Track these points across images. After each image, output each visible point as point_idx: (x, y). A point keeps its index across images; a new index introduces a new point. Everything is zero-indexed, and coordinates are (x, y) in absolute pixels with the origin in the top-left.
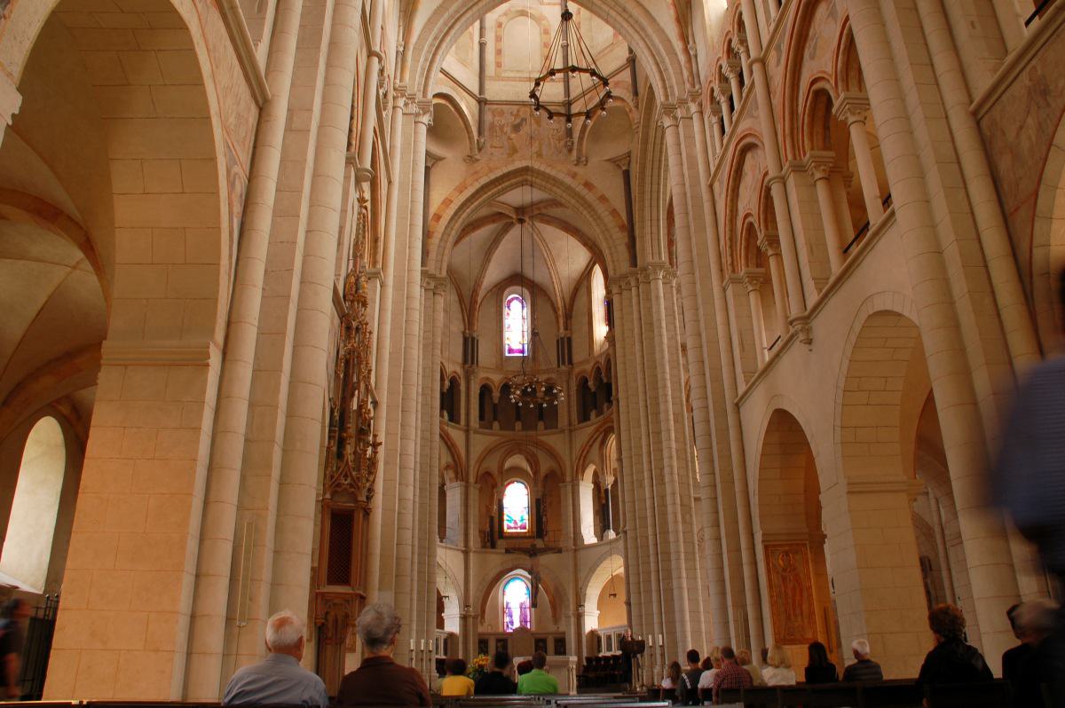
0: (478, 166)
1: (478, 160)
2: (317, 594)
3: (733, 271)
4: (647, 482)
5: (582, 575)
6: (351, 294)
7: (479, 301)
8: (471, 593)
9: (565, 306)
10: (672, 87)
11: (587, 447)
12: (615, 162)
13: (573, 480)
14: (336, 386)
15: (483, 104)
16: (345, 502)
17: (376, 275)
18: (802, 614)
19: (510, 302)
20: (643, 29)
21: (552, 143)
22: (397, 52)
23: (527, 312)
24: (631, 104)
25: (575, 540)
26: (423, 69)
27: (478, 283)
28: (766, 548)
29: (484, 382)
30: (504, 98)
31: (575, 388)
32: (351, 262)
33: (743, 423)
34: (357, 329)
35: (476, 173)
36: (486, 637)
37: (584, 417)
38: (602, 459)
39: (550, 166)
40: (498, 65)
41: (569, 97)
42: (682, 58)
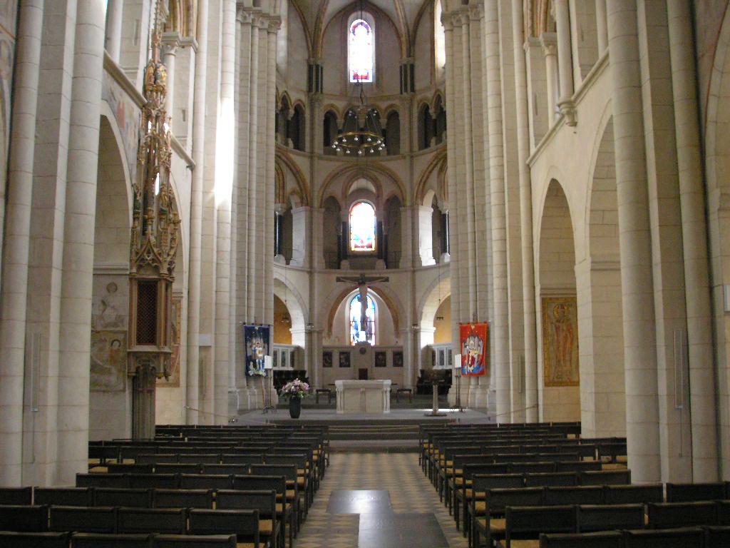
2: (129, 353)
3: (533, 34)
4: (469, 217)
5: (419, 295)
6: (152, 85)
7: (323, 29)
8: (316, 311)
9: (408, 32)
14: (139, 173)
16: (149, 275)
17: (190, 43)
18: (571, 359)
19: (355, 27)
23: (371, 38)
25: (413, 262)
27: (321, 10)
28: (543, 301)
29: (329, 109)
32: (151, 51)
33: (532, 182)
34: (157, 117)
36: (329, 350)
37: (425, 144)
38: (442, 185)
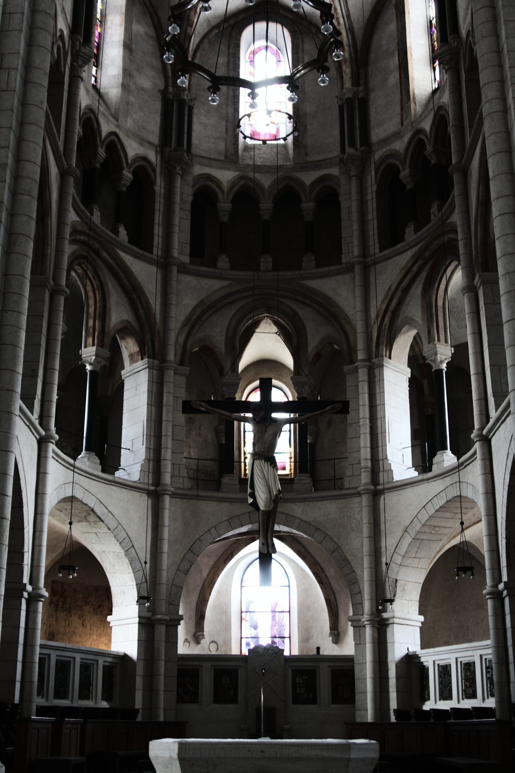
11: (399, 294)
13: (369, 359)
31: (374, 188)
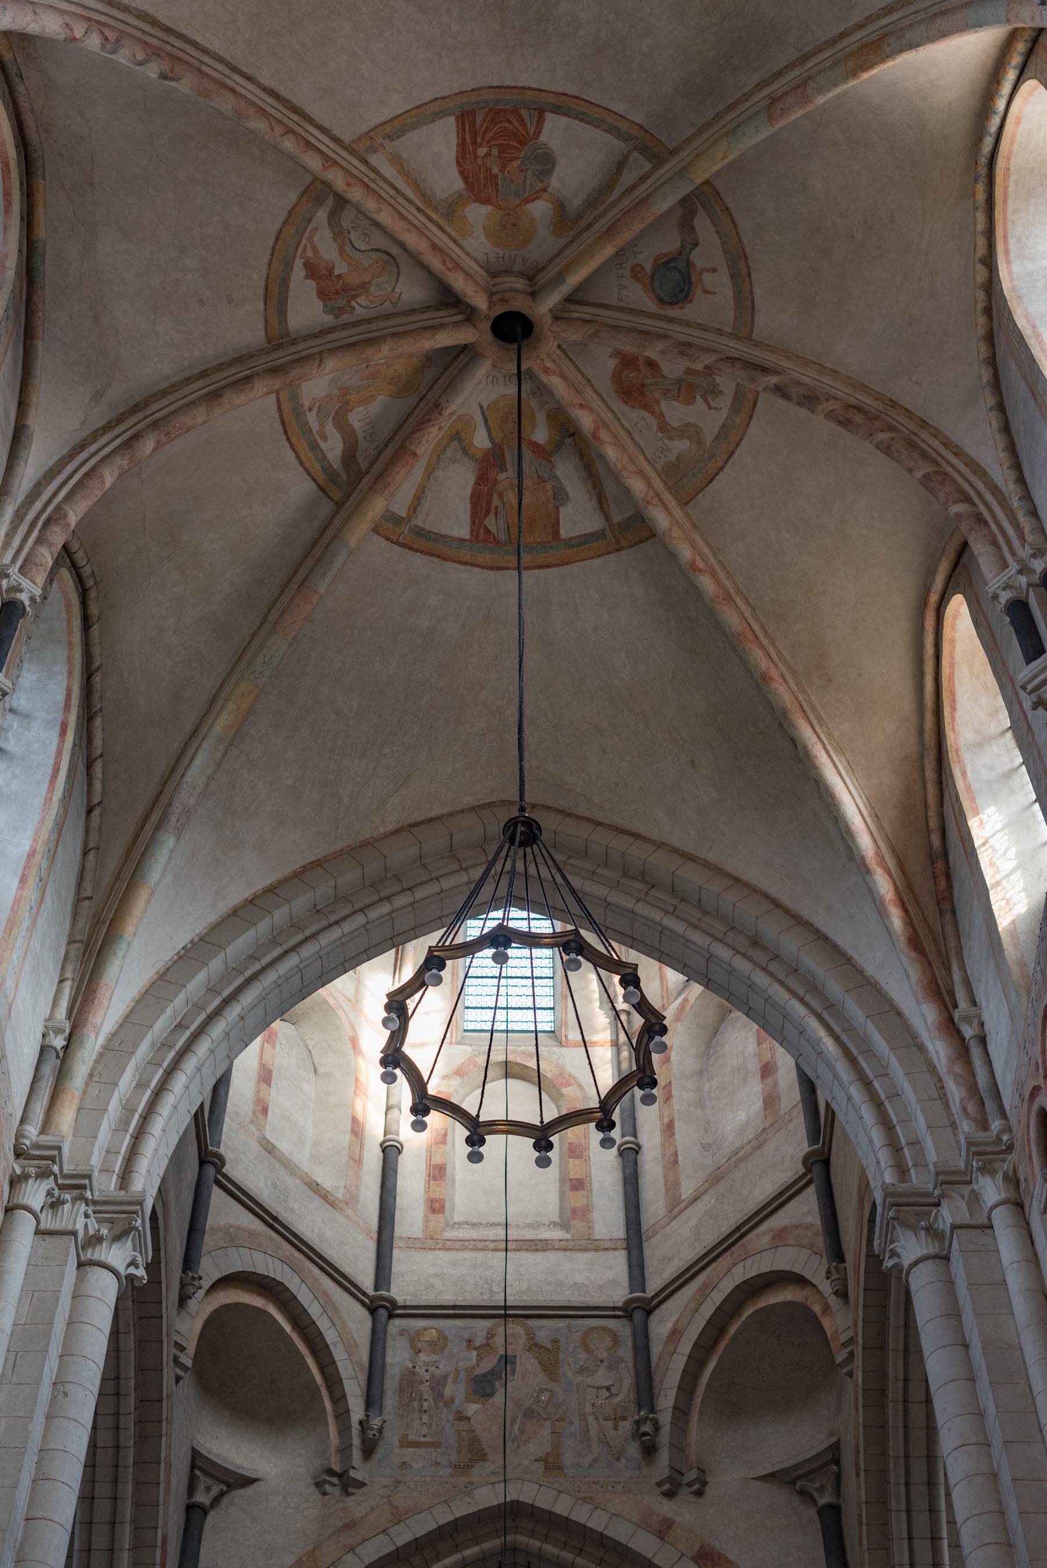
0: (358, 1504)
1: (361, 1485)
10: (915, 1143)
12: (793, 1483)
15: (383, 1314)
20: (815, 989)
21: (594, 1432)
22: (44, 1050)
24: (826, 1287)
26: (128, 1110)
30: (447, 1298)
35: (350, 1525)
39: (584, 1499)
40: (436, 1207)
41: (645, 1293)
42: (939, 1050)
